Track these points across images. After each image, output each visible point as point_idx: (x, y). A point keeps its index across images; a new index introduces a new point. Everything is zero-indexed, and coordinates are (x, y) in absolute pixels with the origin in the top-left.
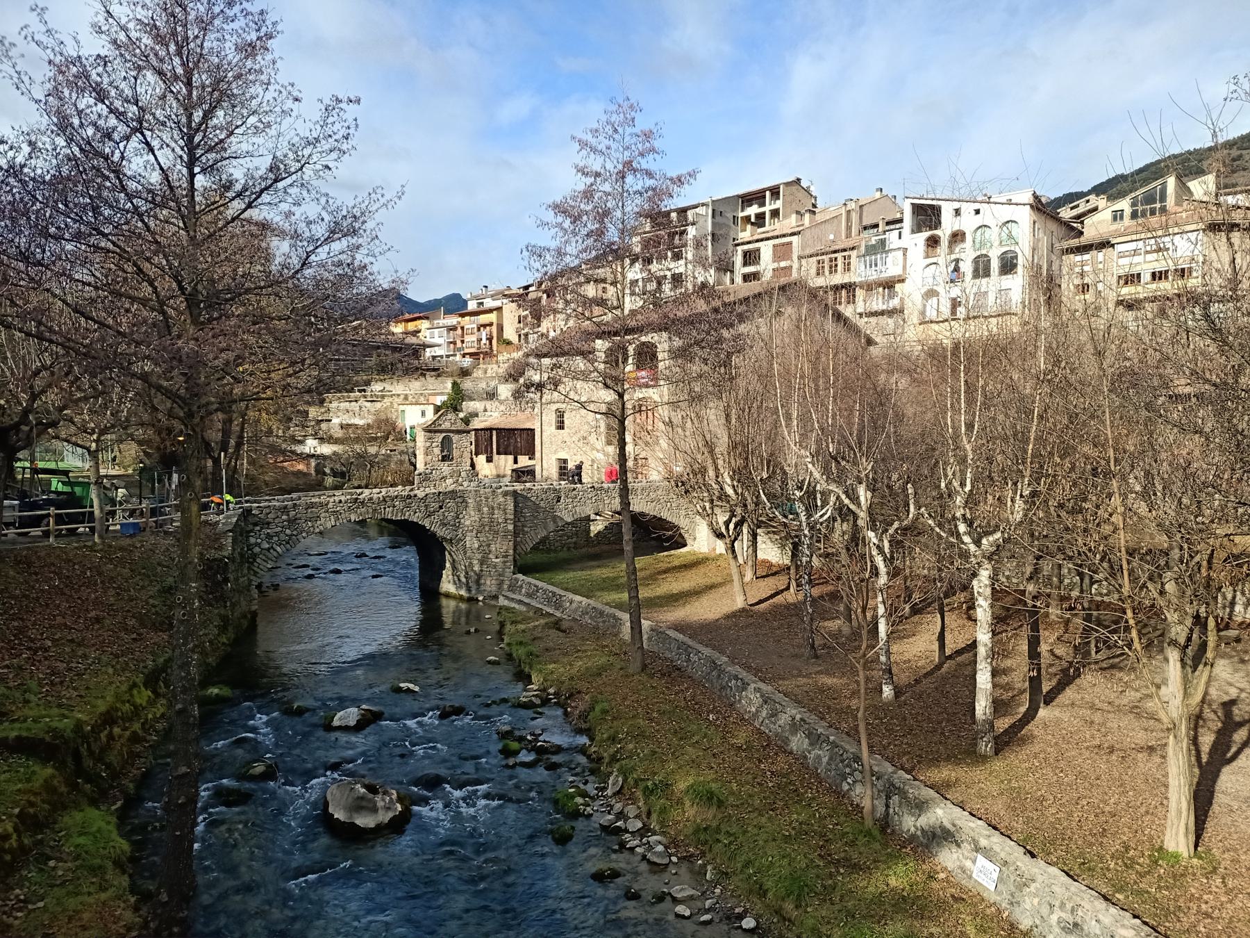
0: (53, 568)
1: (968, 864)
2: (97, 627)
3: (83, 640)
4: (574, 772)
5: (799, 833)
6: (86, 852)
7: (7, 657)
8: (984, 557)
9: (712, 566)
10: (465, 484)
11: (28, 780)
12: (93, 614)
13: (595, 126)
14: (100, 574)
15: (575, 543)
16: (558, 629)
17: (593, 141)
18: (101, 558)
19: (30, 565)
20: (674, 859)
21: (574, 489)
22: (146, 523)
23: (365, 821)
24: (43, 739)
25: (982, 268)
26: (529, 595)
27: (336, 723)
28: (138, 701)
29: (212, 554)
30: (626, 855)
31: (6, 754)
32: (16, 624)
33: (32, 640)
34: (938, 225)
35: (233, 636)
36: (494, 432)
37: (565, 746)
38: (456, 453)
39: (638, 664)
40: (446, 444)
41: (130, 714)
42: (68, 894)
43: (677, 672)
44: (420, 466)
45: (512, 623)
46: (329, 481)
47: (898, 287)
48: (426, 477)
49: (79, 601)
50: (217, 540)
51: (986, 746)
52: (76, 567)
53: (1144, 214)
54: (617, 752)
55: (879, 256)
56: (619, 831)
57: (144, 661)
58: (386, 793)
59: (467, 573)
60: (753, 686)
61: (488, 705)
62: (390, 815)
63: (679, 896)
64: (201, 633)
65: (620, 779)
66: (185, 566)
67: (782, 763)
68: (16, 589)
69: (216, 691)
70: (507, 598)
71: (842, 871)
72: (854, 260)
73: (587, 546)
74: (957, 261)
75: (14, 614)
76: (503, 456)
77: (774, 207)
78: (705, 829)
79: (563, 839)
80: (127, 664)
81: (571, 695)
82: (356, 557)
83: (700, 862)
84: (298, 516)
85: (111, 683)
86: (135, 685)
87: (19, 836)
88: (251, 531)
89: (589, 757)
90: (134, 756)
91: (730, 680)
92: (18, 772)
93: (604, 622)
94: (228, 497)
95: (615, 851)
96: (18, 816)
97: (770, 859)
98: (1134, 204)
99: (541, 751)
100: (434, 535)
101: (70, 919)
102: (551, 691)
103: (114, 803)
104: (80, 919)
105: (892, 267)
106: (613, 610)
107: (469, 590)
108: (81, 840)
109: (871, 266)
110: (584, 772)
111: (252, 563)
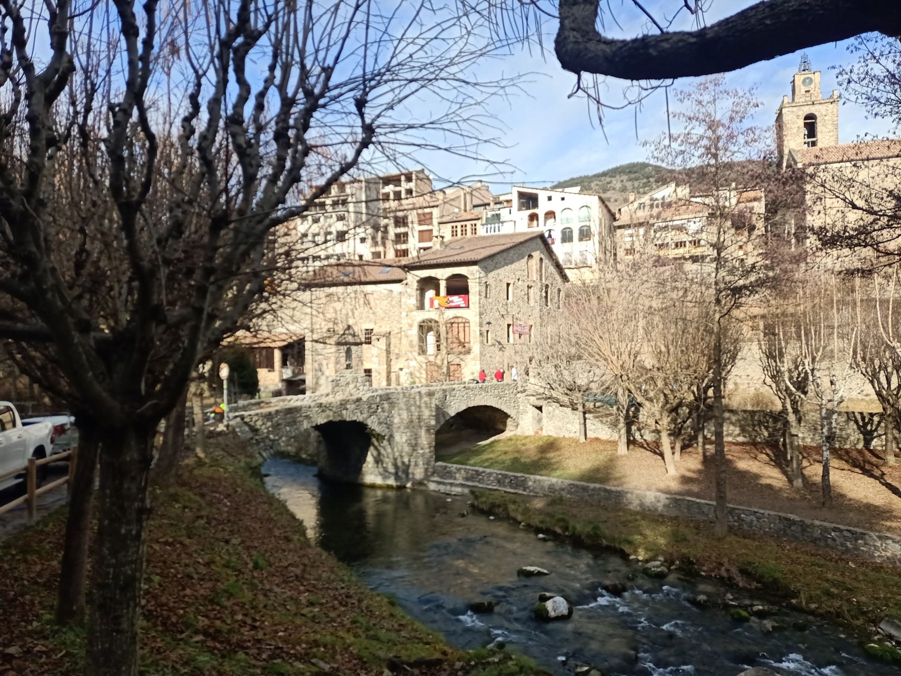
34: (535, 205)
72: (479, 227)
77: (408, 187)
107: (397, 477)
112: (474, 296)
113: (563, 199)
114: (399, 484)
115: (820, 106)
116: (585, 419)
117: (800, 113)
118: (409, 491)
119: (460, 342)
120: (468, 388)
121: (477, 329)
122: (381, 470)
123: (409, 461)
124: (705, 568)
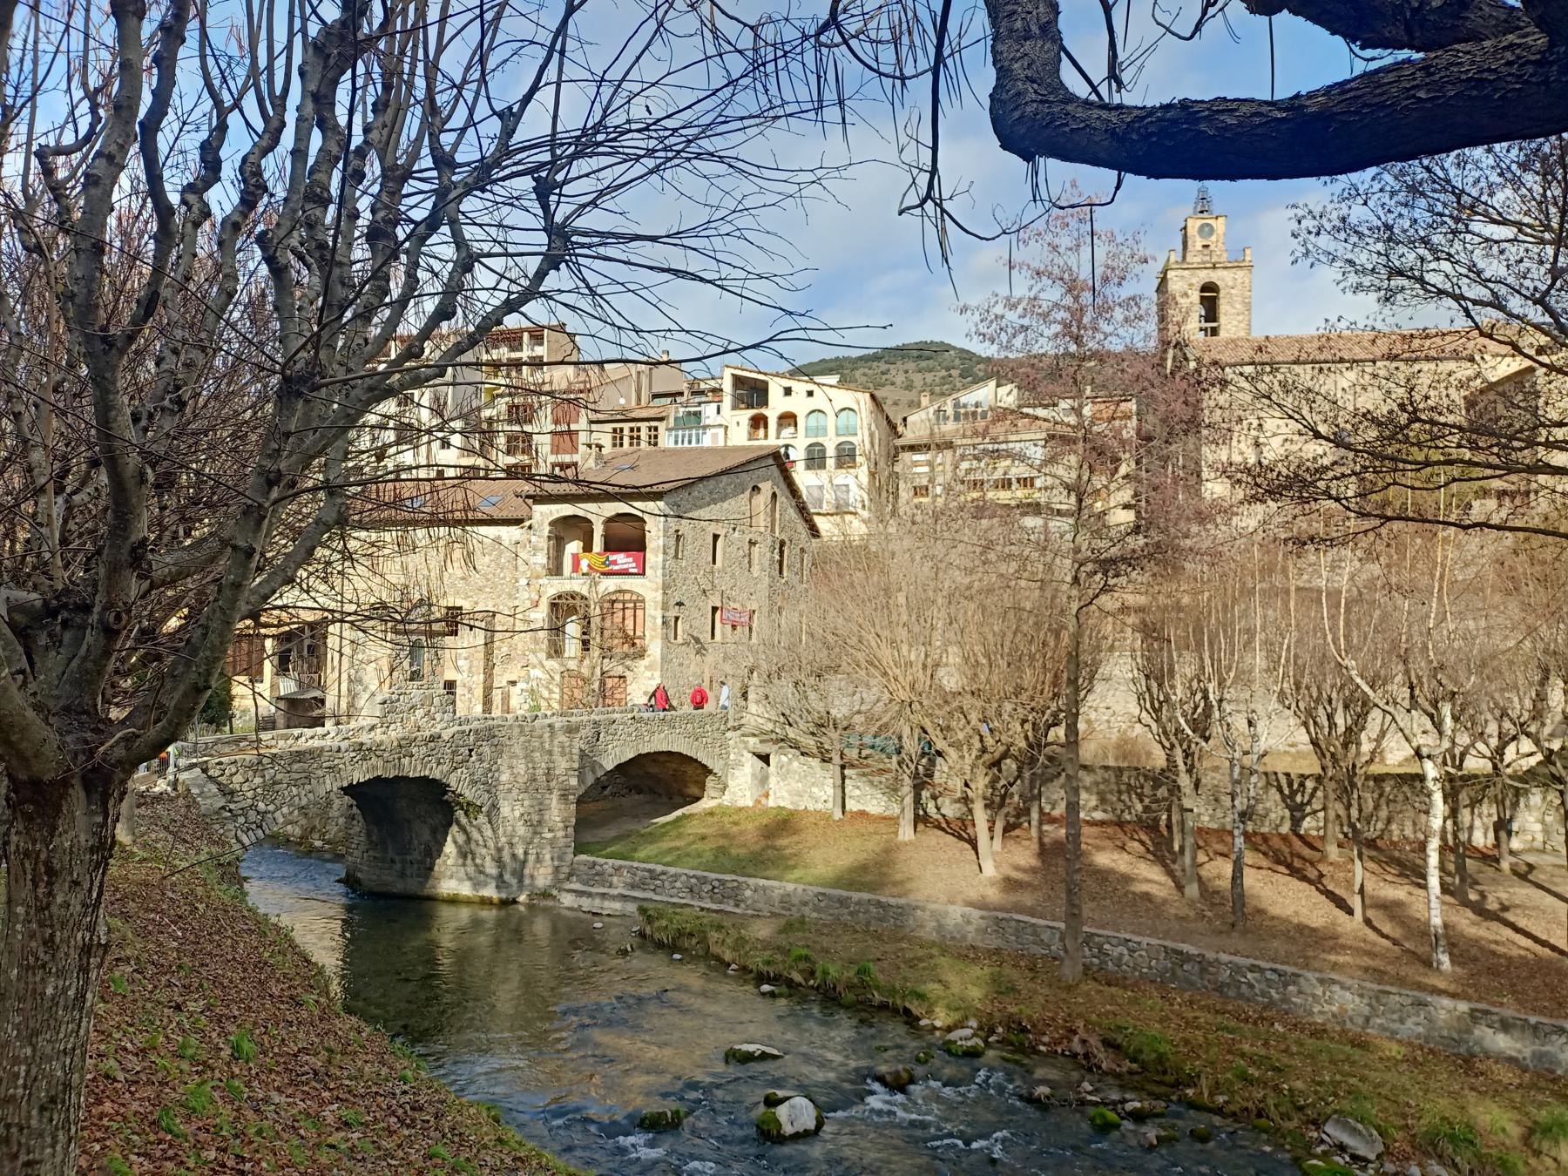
84: (279, 777)
107: (501, 883)
112: (654, 557)
114: (504, 896)
115: (1225, 272)
116: (843, 778)
117: (1194, 281)
118: (522, 908)
119: (626, 636)
120: (641, 720)
121: (659, 614)
122: (471, 869)
123: (526, 853)
124: (1046, 1039)
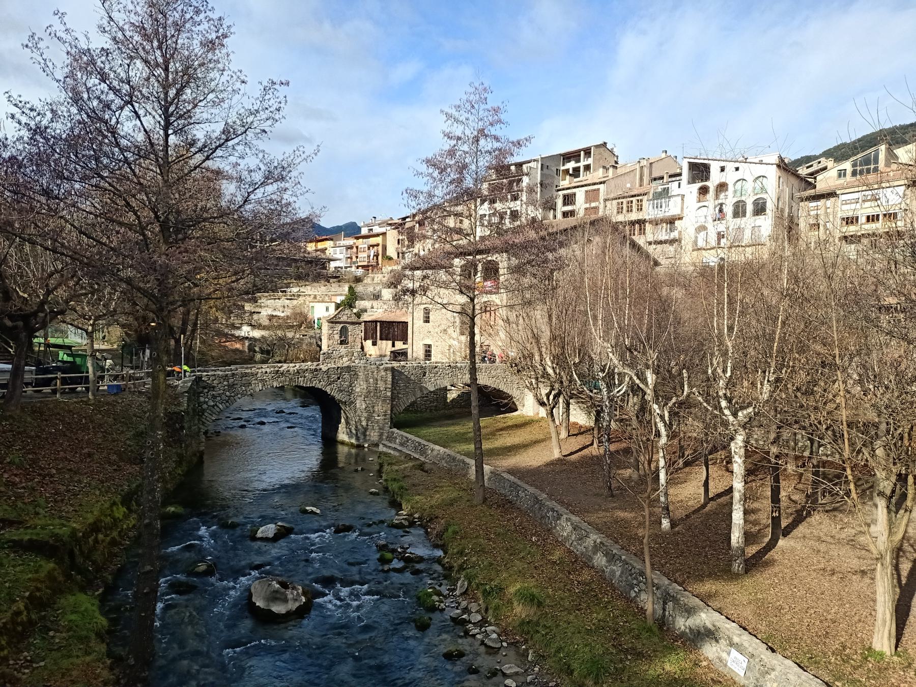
0: (58, 417)
1: (724, 655)
2: (88, 460)
3: (79, 469)
4: (432, 577)
5: (598, 628)
6: (77, 626)
7: (23, 481)
8: (739, 425)
9: (536, 426)
10: (357, 361)
11: (37, 572)
12: (86, 450)
13: (458, 103)
14: (92, 422)
15: (436, 406)
16: (423, 470)
17: (456, 114)
18: (93, 410)
19: (42, 413)
20: (505, 644)
21: (436, 367)
22: (126, 385)
23: (279, 608)
24: (47, 542)
25: (739, 210)
26: (402, 444)
27: (259, 535)
28: (117, 515)
29: (173, 409)
30: (470, 640)
31: (21, 552)
32: (31, 456)
33: (42, 469)
34: (707, 178)
35: (186, 469)
36: (378, 324)
37: (426, 557)
38: (350, 339)
39: (481, 498)
40: (344, 332)
41: (110, 525)
42: (63, 656)
43: (509, 504)
44: (325, 348)
45: (389, 464)
46: (258, 356)
47: (677, 223)
48: (328, 356)
49: (77, 441)
50: (176, 398)
51: (739, 567)
52: (75, 416)
53: (861, 173)
54: (464, 563)
55: (663, 200)
56: (465, 622)
57: (122, 486)
58: (294, 588)
59: (356, 427)
60: (565, 516)
61: (369, 526)
62: (297, 604)
63: (508, 672)
64: (163, 466)
65: (466, 583)
66: (154, 419)
67: (586, 576)
68: (31, 431)
69: (173, 509)
70: (385, 445)
71: (629, 657)
73: (444, 409)
74: (721, 205)
75: (30, 449)
76: (384, 342)
77: (586, 163)
78: (528, 622)
79: (423, 627)
80: (109, 488)
81: (431, 519)
82: (277, 413)
83: (524, 647)
84: (236, 382)
85: (98, 502)
86: (114, 504)
87: (28, 613)
88: (202, 392)
89: (443, 566)
90: (113, 555)
91: (548, 512)
92: (29, 565)
93: (456, 465)
94: (185, 367)
95: (461, 637)
96: (27, 598)
97: (576, 646)
98: (854, 165)
99: (408, 560)
100: (333, 398)
101: (63, 675)
102: (416, 516)
103: (97, 590)
104: (71, 675)
105: (672, 208)
106: (463, 457)
107: (358, 439)
108: (73, 617)
109: (657, 207)
110: (439, 577)
111: (201, 416)
113: (737, 169)
118: (366, 449)
123: (367, 425)
